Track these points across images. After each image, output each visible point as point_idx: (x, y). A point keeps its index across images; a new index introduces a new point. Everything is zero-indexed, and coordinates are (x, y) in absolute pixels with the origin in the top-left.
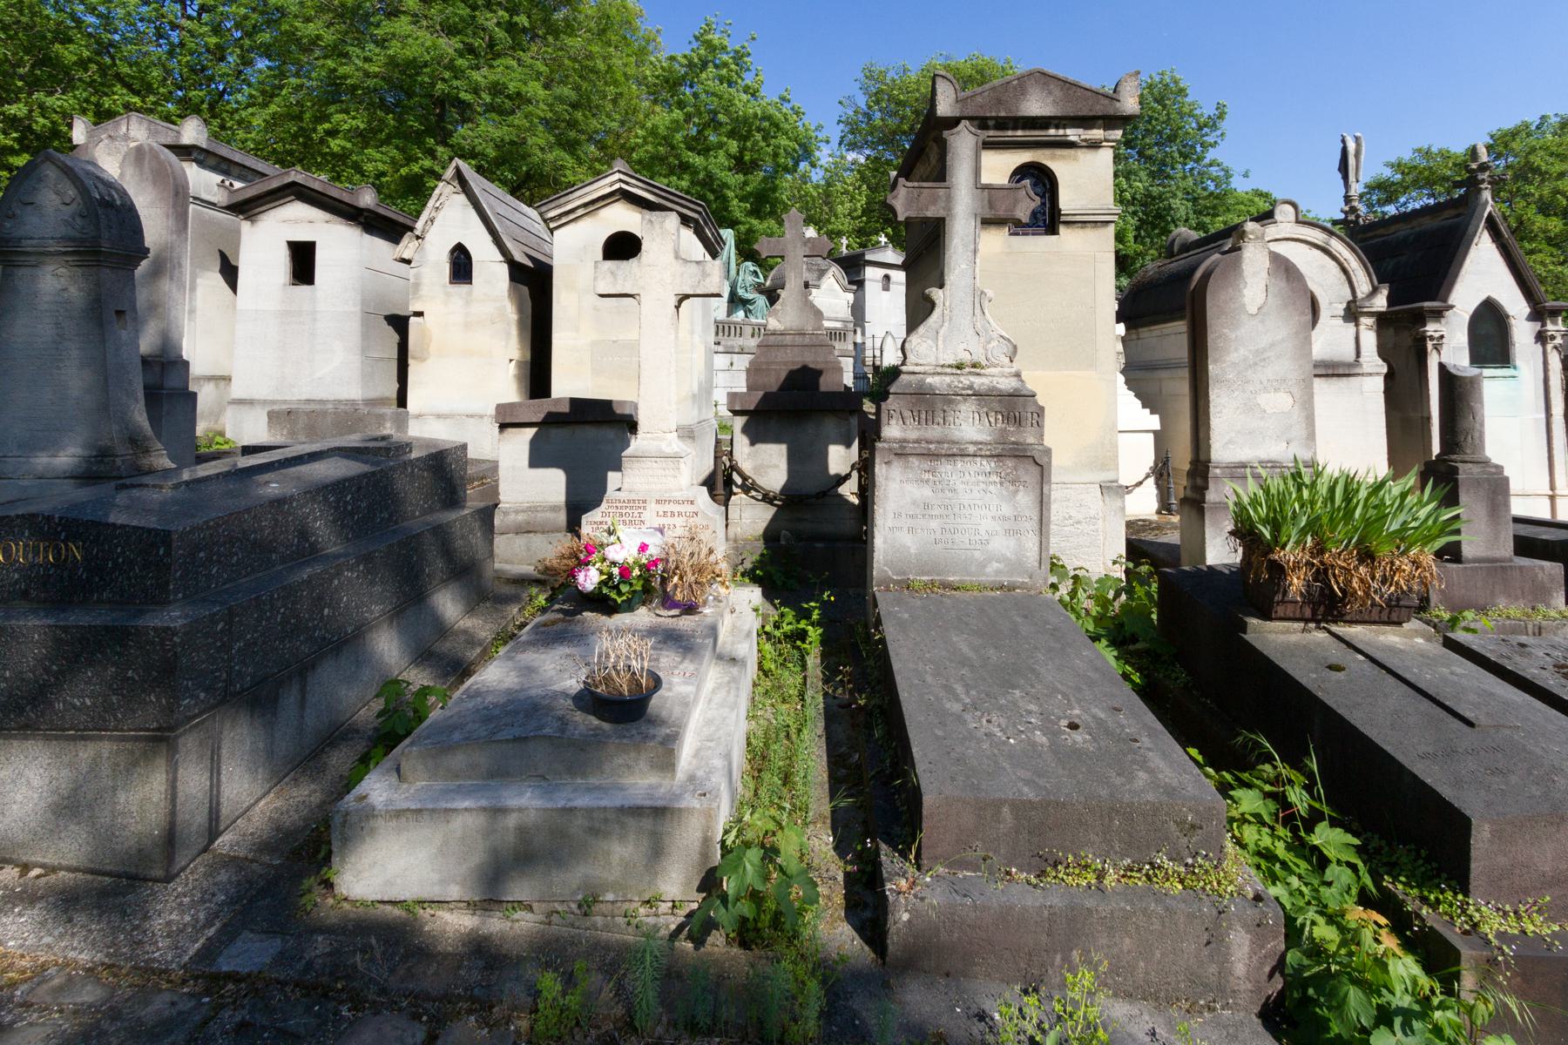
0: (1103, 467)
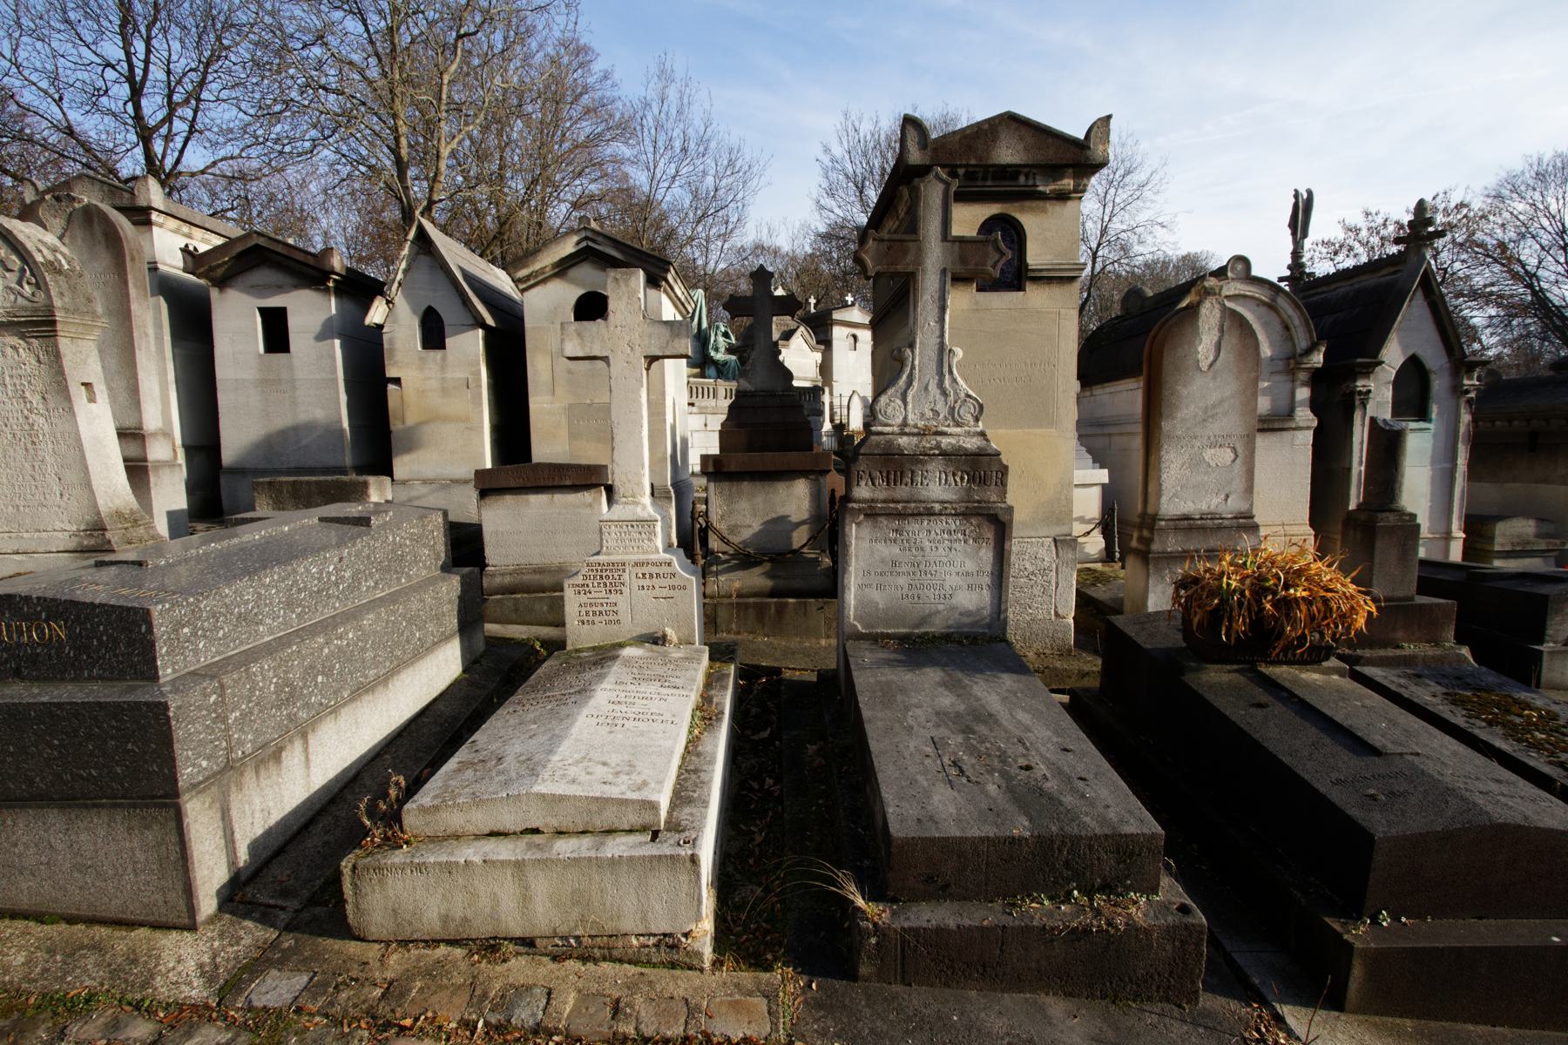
0: (1059, 522)
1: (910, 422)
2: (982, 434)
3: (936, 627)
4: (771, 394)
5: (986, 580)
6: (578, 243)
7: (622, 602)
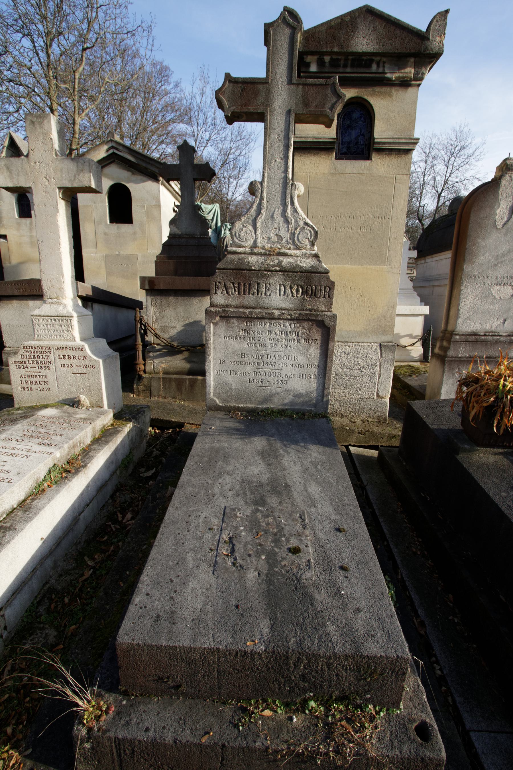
0: (385, 332)
1: (259, 244)
2: (316, 256)
3: (275, 404)
4: (192, 237)
5: (314, 371)
6: (107, 151)
7: (50, 375)
